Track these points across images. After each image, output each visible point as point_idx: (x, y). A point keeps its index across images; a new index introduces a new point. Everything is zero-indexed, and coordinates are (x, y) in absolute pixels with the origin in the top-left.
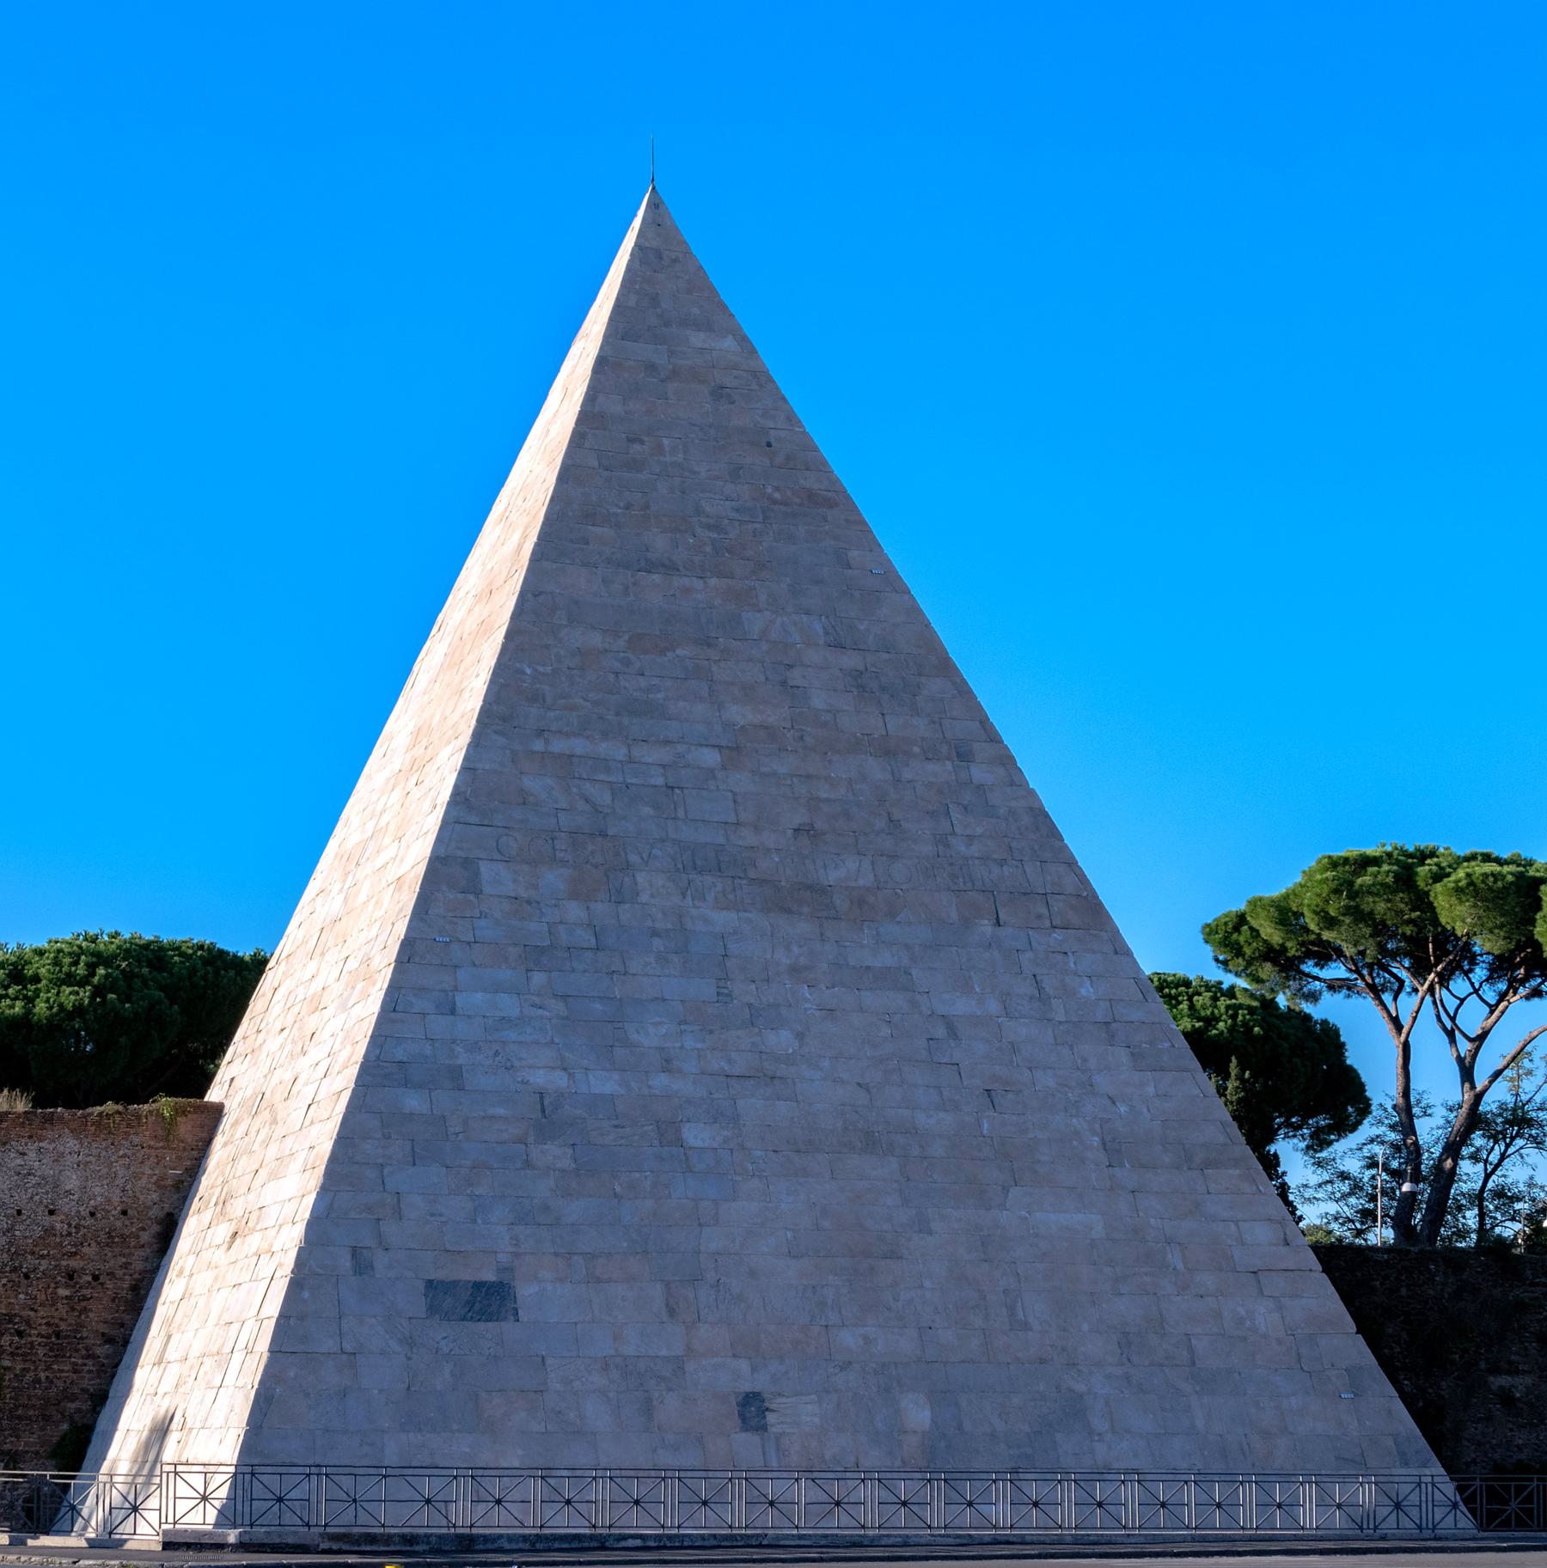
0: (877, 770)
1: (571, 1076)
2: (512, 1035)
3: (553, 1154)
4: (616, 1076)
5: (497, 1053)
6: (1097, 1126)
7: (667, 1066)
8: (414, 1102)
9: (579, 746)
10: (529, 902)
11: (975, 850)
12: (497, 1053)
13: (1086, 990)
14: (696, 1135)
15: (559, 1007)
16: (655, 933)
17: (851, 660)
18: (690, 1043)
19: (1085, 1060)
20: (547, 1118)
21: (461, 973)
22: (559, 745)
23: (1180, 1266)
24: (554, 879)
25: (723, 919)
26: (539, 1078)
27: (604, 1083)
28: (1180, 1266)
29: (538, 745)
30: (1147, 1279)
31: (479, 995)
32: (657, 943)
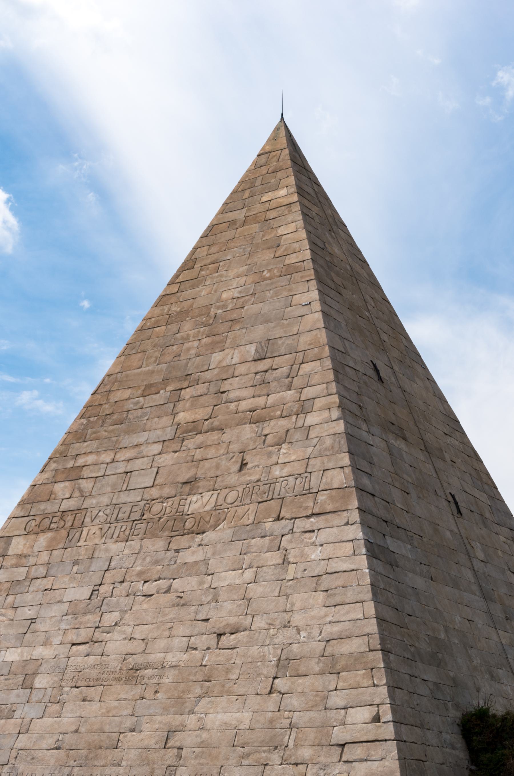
0: (247, 432)
4: (19, 650)
6: (279, 651)
9: (91, 459)
10: (25, 556)
11: (286, 471)
13: (316, 554)
14: (40, 682)
15: (10, 613)
16: (76, 563)
17: (262, 366)
19: (293, 604)
22: (81, 461)
23: (291, 744)
24: (43, 540)
25: (115, 547)
28: (291, 744)
29: (70, 464)
30: (264, 755)
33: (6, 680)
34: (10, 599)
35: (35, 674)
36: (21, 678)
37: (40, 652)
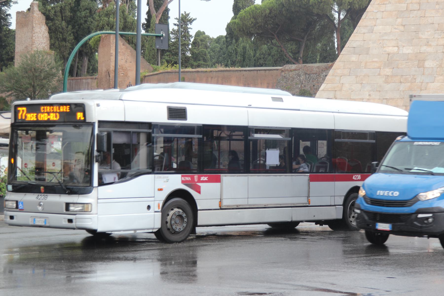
1: (398, 48)
2: (386, 38)
3: (388, 71)
4: (411, 48)
5: (380, 43)
7: (428, 44)
8: (354, 58)
12: (380, 43)
14: (428, 64)
15: (402, 28)
18: (436, 36)
20: (390, 61)
21: (378, 21)
26: (390, 49)
27: (408, 50)
31: (381, 27)
32: (437, 7)
33: (406, 62)
34: (399, 20)
35: (424, 60)
36: (416, 63)
37: (424, 49)
